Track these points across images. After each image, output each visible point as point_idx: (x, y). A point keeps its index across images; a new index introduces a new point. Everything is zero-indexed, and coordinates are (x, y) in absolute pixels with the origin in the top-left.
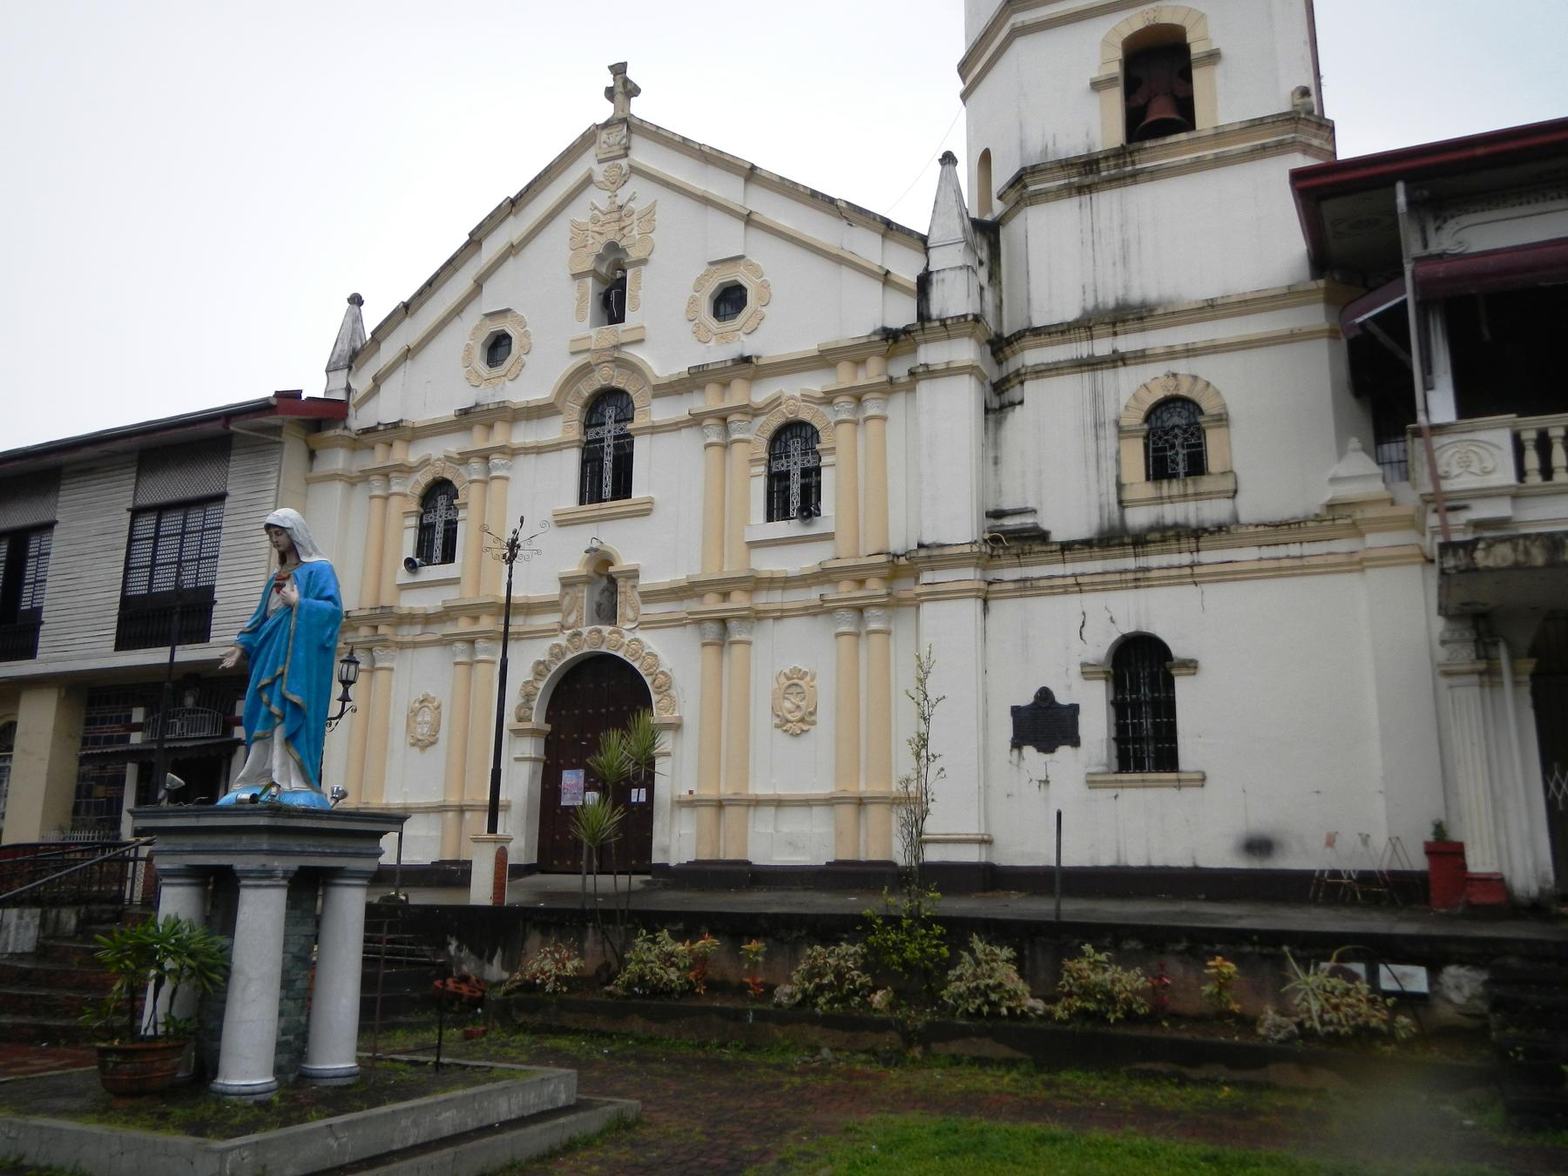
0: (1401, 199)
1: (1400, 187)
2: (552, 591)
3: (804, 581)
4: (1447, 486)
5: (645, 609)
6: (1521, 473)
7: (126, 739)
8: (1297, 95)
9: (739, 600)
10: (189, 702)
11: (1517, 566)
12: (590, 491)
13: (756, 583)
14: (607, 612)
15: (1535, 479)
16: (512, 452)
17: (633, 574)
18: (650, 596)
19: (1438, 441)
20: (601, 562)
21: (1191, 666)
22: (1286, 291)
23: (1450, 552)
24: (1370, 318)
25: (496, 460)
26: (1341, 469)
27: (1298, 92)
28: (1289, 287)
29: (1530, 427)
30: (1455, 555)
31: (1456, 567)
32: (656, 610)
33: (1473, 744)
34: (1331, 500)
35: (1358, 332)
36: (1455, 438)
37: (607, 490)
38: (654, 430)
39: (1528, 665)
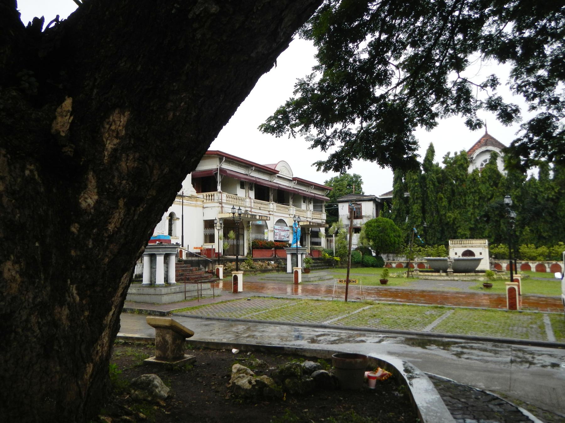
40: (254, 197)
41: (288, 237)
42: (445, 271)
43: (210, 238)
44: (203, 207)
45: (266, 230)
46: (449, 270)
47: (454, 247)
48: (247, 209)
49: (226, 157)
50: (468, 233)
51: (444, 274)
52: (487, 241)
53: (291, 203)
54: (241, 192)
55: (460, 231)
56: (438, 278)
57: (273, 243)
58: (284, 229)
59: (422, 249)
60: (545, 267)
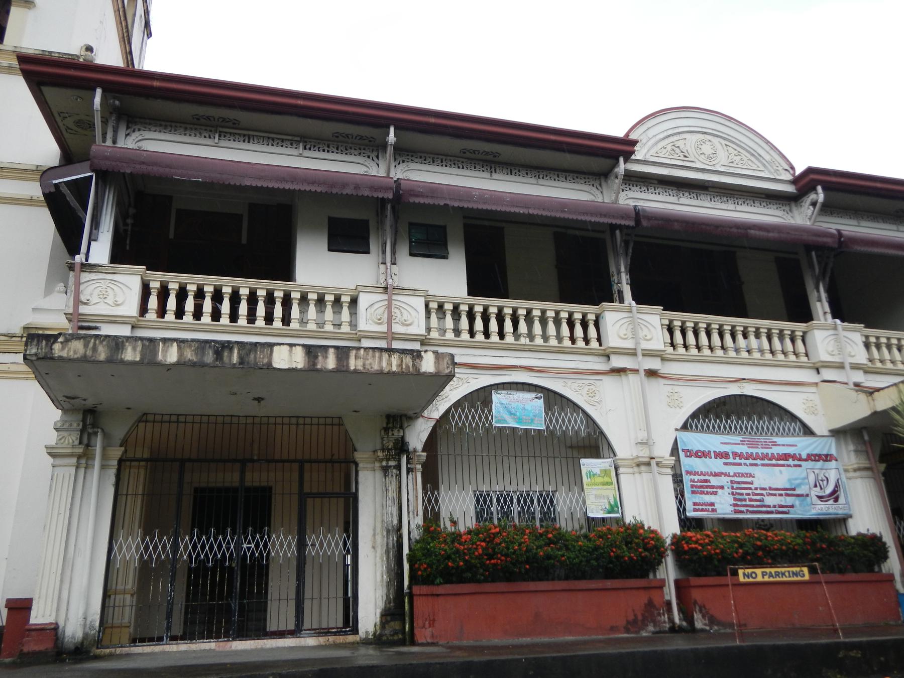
0: (98, 99)
1: (99, 92)
4: (83, 309)
6: (143, 310)
8: (84, 49)
11: (84, 359)
15: (152, 316)
19: (85, 276)
22: (34, 168)
23: (35, 342)
24: (64, 182)
26: (44, 303)
27: (85, 48)
28: (37, 166)
29: (156, 279)
30: (38, 345)
31: (36, 354)
33: (59, 514)
34: (28, 324)
35: (53, 190)
36: (101, 276)
39: (117, 452)
41: (834, 495)
58: (776, 450)
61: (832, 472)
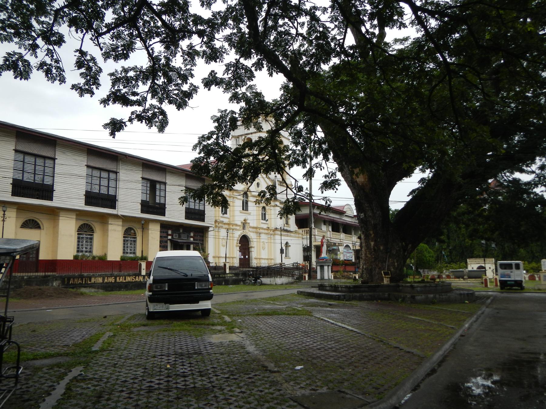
2: (239, 223)
3: (265, 229)
5: (250, 229)
7: (167, 237)
9: (261, 231)
10: (181, 231)
12: (243, 209)
13: (263, 229)
14: (244, 228)
16: (236, 198)
17: (249, 223)
18: (251, 227)
20: (245, 220)
21: (290, 246)
25: (235, 199)
32: (251, 229)
37: (245, 209)
38: (251, 201)
40: (331, 230)
42: (463, 278)
43: (307, 258)
44: (303, 238)
45: (339, 253)
46: (465, 277)
47: (471, 264)
48: (328, 238)
49: (317, 206)
50: (481, 254)
51: (462, 279)
52: (493, 259)
53: (353, 233)
54: (324, 228)
55: (475, 252)
56: (459, 282)
57: (344, 262)
59: (449, 265)
60: (535, 277)
61: (352, 254)
